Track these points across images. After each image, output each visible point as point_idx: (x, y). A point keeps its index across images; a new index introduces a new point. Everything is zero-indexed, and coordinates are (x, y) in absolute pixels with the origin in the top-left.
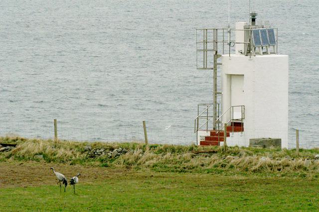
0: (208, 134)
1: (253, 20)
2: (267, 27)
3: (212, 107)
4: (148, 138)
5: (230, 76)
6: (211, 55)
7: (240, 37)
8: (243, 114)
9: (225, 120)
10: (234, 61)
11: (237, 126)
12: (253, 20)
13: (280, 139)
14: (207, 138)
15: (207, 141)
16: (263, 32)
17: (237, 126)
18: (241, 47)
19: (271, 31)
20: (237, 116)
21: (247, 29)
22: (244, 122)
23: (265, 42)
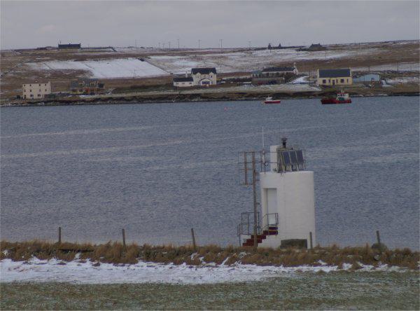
0: (249, 237)
1: (284, 144)
2: (296, 149)
3: (252, 215)
4: (196, 241)
5: (267, 190)
6: (250, 173)
7: (273, 157)
8: (277, 219)
9: (264, 228)
10: (270, 179)
11: (273, 231)
12: (284, 144)
13: (282, 241)
14: (248, 241)
15: (250, 243)
16: (293, 154)
17: (273, 231)
18: (274, 166)
19: (300, 153)
20: (272, 222)
21: (279, 151)
22: (278, 226)
23: (294, 160)
